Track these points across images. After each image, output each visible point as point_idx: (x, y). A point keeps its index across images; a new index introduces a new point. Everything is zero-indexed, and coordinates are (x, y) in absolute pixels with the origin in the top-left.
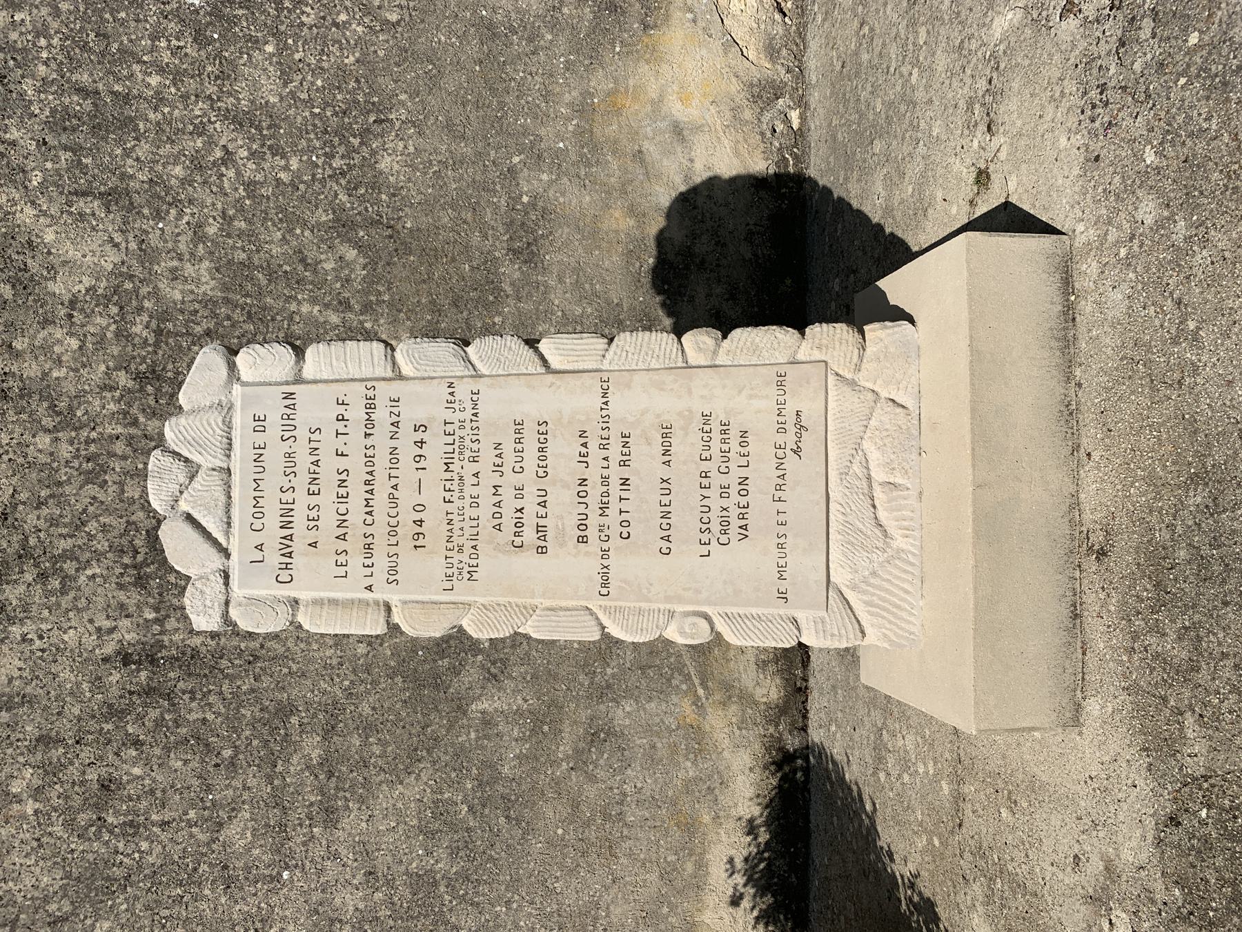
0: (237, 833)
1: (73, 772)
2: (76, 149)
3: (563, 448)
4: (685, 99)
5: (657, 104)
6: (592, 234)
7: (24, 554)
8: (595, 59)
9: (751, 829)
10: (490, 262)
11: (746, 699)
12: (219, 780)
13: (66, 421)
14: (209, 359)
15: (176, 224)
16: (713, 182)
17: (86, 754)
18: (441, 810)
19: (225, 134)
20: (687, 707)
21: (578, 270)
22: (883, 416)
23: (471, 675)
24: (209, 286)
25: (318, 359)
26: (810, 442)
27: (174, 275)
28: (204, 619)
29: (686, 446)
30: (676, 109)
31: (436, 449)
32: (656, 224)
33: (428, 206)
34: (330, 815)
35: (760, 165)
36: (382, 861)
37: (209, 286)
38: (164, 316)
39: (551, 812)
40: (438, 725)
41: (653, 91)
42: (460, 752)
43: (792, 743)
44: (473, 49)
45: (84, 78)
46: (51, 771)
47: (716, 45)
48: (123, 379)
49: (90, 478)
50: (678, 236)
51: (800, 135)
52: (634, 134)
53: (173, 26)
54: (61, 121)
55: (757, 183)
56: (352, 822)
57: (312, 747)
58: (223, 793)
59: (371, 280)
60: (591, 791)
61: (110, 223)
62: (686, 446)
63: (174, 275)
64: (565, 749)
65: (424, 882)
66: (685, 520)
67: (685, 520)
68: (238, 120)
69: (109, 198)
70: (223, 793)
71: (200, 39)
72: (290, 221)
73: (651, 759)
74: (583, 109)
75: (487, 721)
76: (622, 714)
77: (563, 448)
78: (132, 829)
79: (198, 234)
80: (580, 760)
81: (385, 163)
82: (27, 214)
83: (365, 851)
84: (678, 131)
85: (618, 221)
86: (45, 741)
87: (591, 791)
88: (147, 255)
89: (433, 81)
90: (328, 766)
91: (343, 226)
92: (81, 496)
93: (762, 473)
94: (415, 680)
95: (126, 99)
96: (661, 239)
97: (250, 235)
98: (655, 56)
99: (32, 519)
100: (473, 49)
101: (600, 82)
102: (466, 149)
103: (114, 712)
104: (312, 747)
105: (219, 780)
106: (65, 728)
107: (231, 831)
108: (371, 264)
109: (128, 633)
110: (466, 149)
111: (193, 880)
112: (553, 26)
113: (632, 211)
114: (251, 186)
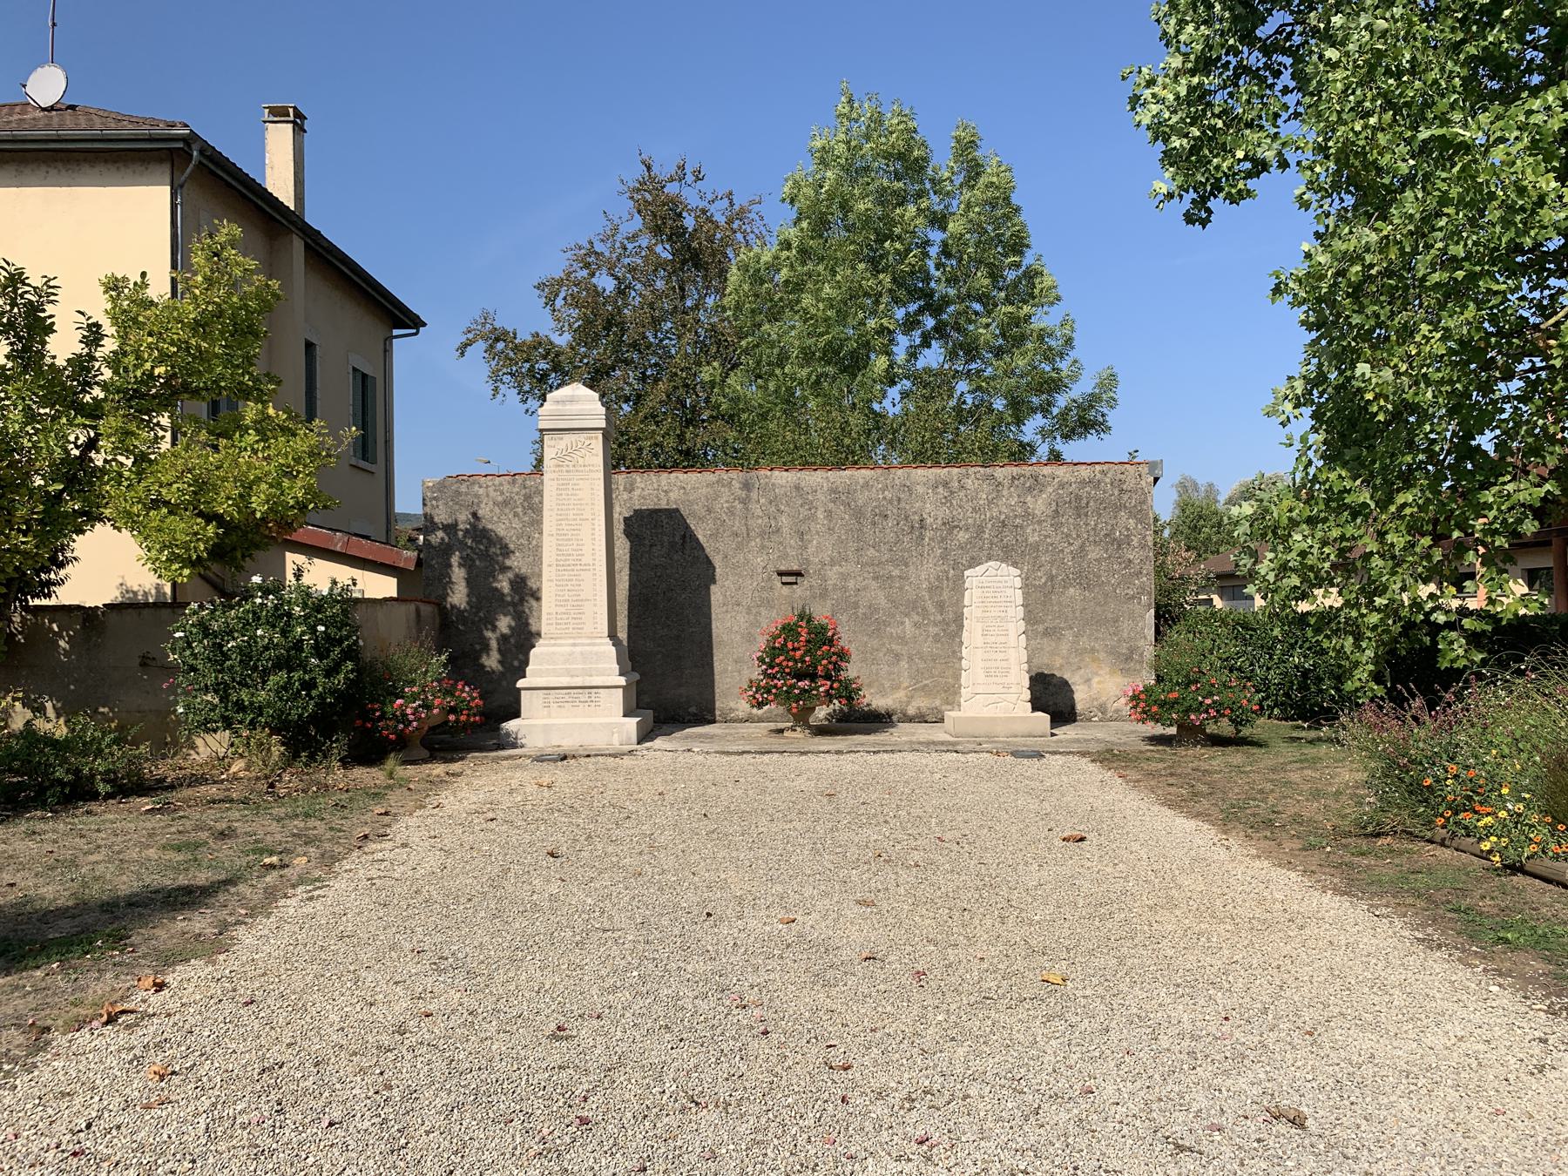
0: (871, 553)
1: (890, 507)
2: (1070, 502)
3: (1003, 639)
4: (1099, 683)
5: (1097, 674)
6: (1053, 653)
7: (952, 493)
8: (1110, 653)
9: (868, 705)
10: (1044, 621)
11: (908, 703)
12: (887, 547)
13: (990, 502)
14: (1019, 572)
15: (1050, 531)
16: (1072, 691)
17: (895, 511)
18: (877, 610)
19: (1077, 543)
20: (906, 684)
21: (1042, 649)
22: (1012, 706)
23: (916, 618)
24: (1031, 540)
25: (1019, 592)
26: (1005, 690)
27: (1034, 530)
28: (967, 573)
29: (1004, 664)
30: (1096, 680)
31: (1003, 614)
32: (1058, 674)
33: (1060, 603)
34: (876, 578)
35: (1079, 707)
36: (863, 593)
37: (1031, 540)
38: (1022, 527)
39: (875, 643)
40: (902, 608)
41: (1101, 672)
42: (893, 616)
43: (895, 718)
44: (1110, 616)
45: (1092, 504)
46: (890, 502)
47: (1118, 693)
48: (1003, 517)
49: (974, 509)
50: (1054, 681)
51: (1089, 720)
52: (1086, 666)
53: (1109, 527)
54: (1078, 498)
55: (1073, 707)
56: (874, 584)
57: (896, 572)
58: (884, 548)
59: (1035, 586)
60: (881, 655)
61: (1049, 512)
62: (1004, 664)
63: (1034, 530)
64: (894, 647)
65: (856, 605)
66: (989, 664)
67: (989, 664)
68: (1082, 547)
69: (1056, 511)
70: (884, 548)
71: (1106, 535)
72: (1052, 563)
73: (890, 673)
74: (1093, 650)
75: (903, 623)
76: (904, 664)
77: (1003, 639)
78: (874, 524)
79: (1046, 537)
80: (890, 651)
81: (1072, 590)
82: (1050, 489)
83: (866, 588)
84: (1088, 681)
85: (1058, 662)
86: (899, 500)
87: (881, 655)
88: (1040, 522)
89: (1098, 604)
90: (890, 577)
91: (1052, 578)
92: (969, 506)
93: (999, 680)
94: (915, 601)
95: (1086, 515)
96: (1053, 675)
97: (1047, 551)
98: (1112, 673)
99: (962, 494)
100: (1110, 616)
101: (1102, 655)
102: (1078, 614)
103: (906, 518)
104: (896, 572)
105: (887, 547)
106: (903, 505)
107: (872, 550)
108: (1040, 586)
109: (929, 521)
110: (1078, 614)
111: (859, 540)
112: (1119, 641)
113: (1062, 666)
114: (1062, 551)
